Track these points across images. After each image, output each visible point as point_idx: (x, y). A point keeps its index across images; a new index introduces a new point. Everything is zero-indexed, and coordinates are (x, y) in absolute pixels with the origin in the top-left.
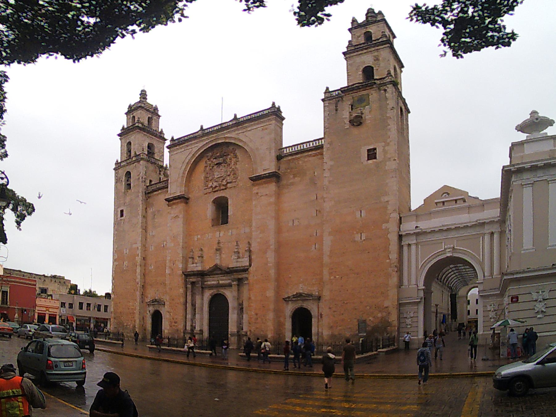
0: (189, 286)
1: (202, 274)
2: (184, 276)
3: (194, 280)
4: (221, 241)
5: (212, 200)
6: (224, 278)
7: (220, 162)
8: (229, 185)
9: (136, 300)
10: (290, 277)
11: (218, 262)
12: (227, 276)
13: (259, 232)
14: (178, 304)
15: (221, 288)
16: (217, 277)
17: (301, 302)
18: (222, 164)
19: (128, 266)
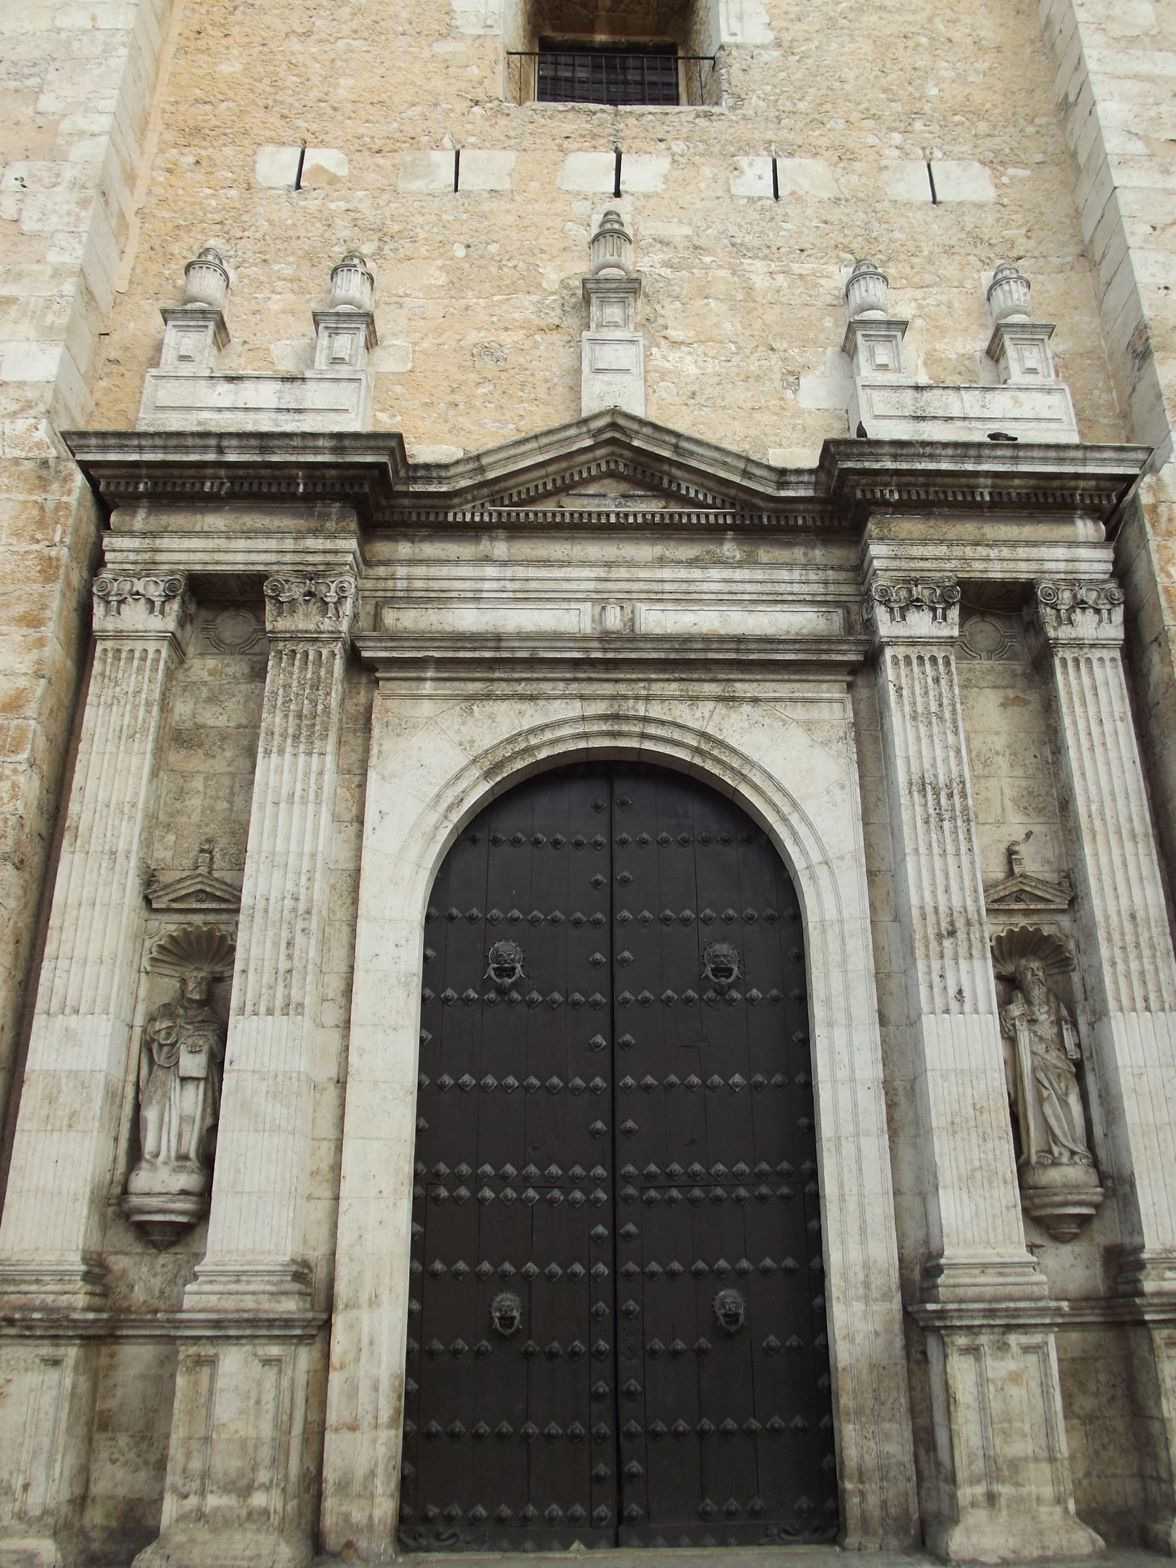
0: (135, 617)
2: (79, 478)
12: (750, 562)
15: (673, 688)
16: (608, 565)
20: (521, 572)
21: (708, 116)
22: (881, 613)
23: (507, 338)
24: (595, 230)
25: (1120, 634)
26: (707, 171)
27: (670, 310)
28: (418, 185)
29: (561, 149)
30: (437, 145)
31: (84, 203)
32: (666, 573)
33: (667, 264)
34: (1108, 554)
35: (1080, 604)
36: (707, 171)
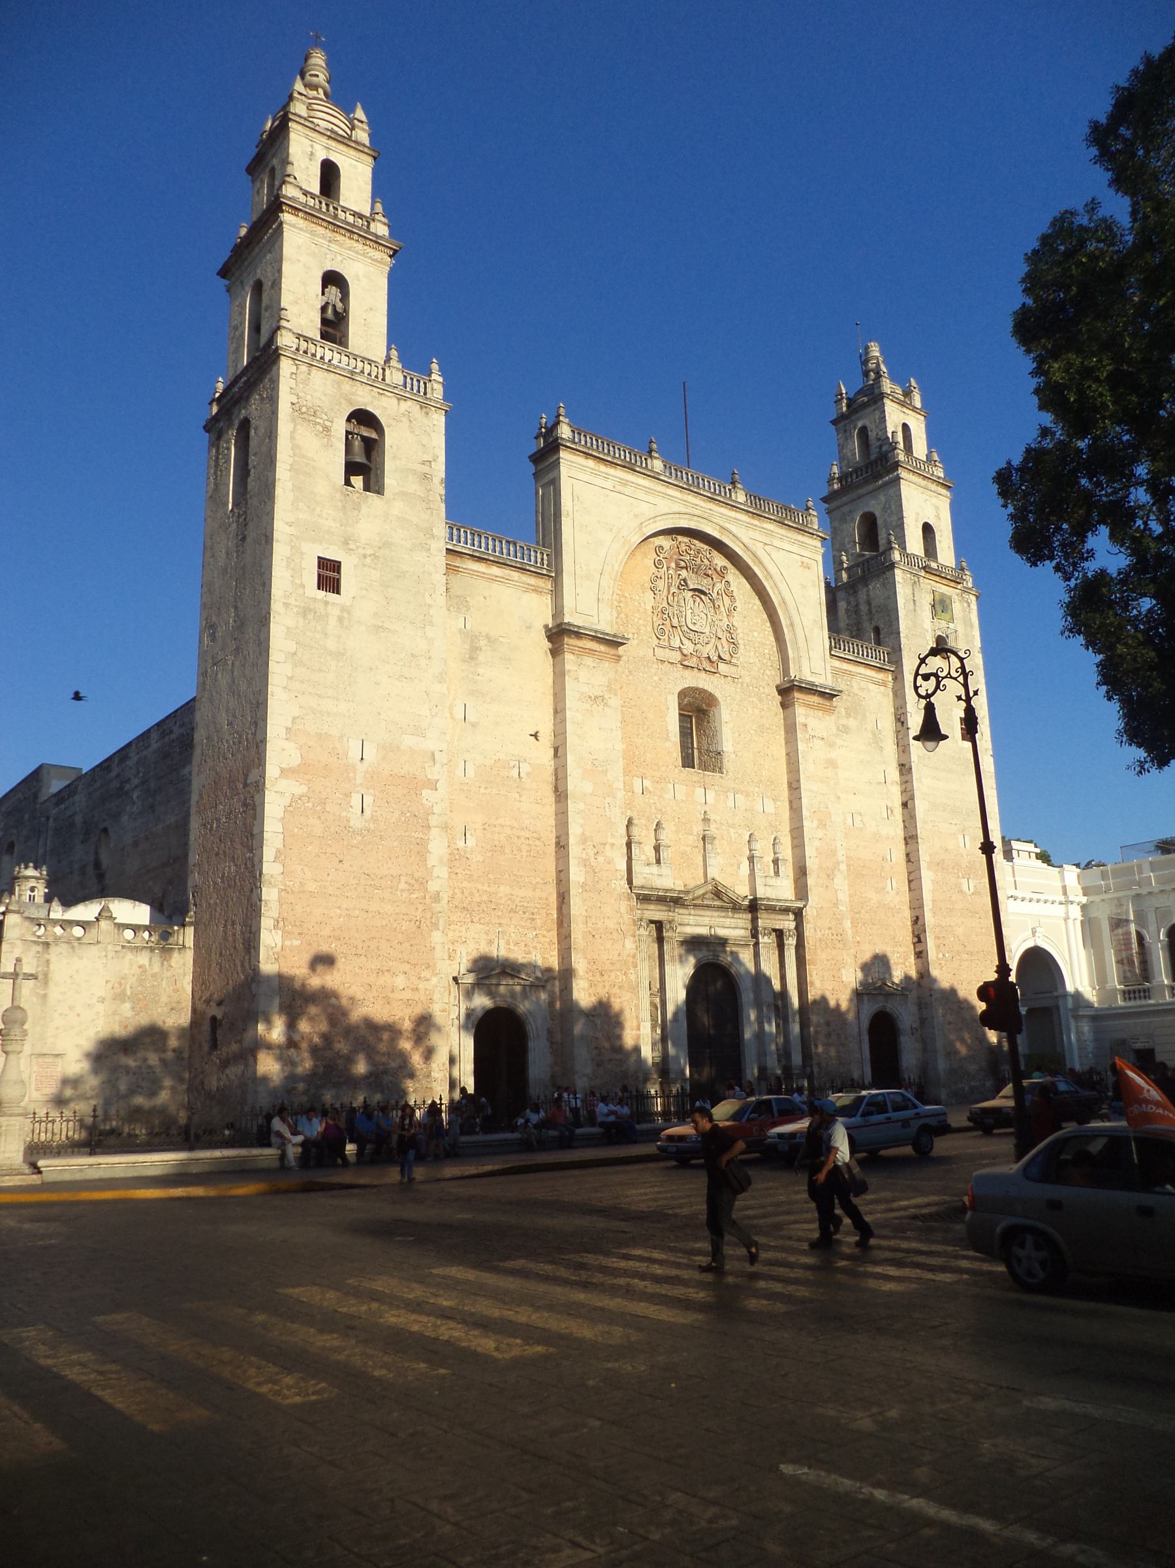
1: (675, 901)
3: (657, 916)
4: (711, 816)
5: (679, 689)
6: (728, 922)
7: (704, 589)
8: (722, 667)
9: (428, 967)
10: (858, 942)
11: (713, 873)
12: (733, 918)
13: (816, 823)
14: (620, 987)
17: (881, 998)
18: (703, 597)
19: (374, 819)
20: (697, 918)
21: (721, 777)
22: (760, 936)
23: (688, 849)
24: (703, 817)
25: (795, 942)
26: (722, 797)
27: (716, 842)
28: (667, 796)
29: (694, 786)
30: (669, 782)
31: (622, 813)
32: (723, 920)
33: (716, 829)
34: (794, 923)
35: (790, 936)
36: (722, 797)
